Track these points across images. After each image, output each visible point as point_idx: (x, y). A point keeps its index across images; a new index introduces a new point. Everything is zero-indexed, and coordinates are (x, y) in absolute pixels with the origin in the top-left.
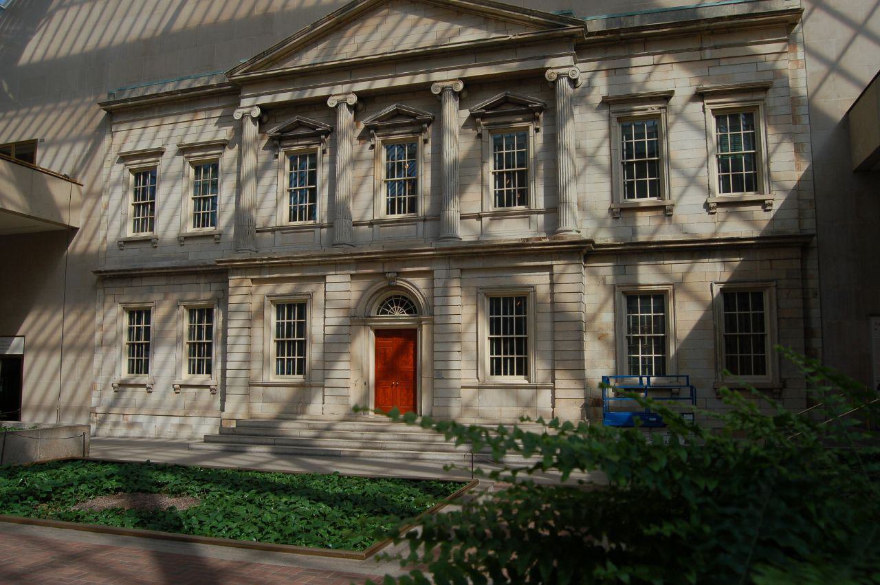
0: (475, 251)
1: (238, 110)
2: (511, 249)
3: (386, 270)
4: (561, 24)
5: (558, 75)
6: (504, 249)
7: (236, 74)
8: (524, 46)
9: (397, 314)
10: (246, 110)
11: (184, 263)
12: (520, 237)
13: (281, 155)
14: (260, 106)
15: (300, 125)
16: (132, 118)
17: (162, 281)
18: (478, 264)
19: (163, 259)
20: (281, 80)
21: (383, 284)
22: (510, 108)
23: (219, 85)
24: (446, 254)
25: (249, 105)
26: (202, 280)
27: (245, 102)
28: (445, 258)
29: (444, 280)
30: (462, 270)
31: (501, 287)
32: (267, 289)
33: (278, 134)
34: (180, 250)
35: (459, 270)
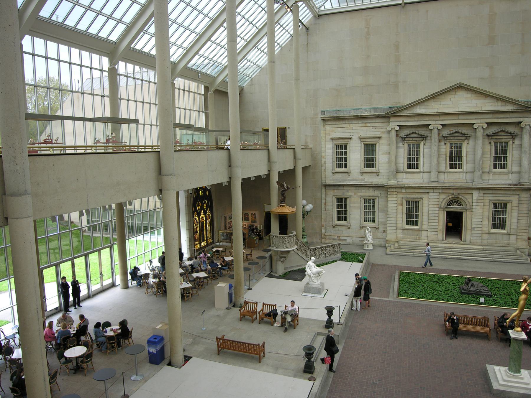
3: (454, 192)
7: (390, 114)
9: (455, 206)
10: (393, 127)
16: (334, 123)
17: (353, 188)
19: (353, 180)
21: (453, 196)
22: (503, 133)
25: (395, 124)
26: (371, 189)
32: (401, 196)
34: (360, 177)
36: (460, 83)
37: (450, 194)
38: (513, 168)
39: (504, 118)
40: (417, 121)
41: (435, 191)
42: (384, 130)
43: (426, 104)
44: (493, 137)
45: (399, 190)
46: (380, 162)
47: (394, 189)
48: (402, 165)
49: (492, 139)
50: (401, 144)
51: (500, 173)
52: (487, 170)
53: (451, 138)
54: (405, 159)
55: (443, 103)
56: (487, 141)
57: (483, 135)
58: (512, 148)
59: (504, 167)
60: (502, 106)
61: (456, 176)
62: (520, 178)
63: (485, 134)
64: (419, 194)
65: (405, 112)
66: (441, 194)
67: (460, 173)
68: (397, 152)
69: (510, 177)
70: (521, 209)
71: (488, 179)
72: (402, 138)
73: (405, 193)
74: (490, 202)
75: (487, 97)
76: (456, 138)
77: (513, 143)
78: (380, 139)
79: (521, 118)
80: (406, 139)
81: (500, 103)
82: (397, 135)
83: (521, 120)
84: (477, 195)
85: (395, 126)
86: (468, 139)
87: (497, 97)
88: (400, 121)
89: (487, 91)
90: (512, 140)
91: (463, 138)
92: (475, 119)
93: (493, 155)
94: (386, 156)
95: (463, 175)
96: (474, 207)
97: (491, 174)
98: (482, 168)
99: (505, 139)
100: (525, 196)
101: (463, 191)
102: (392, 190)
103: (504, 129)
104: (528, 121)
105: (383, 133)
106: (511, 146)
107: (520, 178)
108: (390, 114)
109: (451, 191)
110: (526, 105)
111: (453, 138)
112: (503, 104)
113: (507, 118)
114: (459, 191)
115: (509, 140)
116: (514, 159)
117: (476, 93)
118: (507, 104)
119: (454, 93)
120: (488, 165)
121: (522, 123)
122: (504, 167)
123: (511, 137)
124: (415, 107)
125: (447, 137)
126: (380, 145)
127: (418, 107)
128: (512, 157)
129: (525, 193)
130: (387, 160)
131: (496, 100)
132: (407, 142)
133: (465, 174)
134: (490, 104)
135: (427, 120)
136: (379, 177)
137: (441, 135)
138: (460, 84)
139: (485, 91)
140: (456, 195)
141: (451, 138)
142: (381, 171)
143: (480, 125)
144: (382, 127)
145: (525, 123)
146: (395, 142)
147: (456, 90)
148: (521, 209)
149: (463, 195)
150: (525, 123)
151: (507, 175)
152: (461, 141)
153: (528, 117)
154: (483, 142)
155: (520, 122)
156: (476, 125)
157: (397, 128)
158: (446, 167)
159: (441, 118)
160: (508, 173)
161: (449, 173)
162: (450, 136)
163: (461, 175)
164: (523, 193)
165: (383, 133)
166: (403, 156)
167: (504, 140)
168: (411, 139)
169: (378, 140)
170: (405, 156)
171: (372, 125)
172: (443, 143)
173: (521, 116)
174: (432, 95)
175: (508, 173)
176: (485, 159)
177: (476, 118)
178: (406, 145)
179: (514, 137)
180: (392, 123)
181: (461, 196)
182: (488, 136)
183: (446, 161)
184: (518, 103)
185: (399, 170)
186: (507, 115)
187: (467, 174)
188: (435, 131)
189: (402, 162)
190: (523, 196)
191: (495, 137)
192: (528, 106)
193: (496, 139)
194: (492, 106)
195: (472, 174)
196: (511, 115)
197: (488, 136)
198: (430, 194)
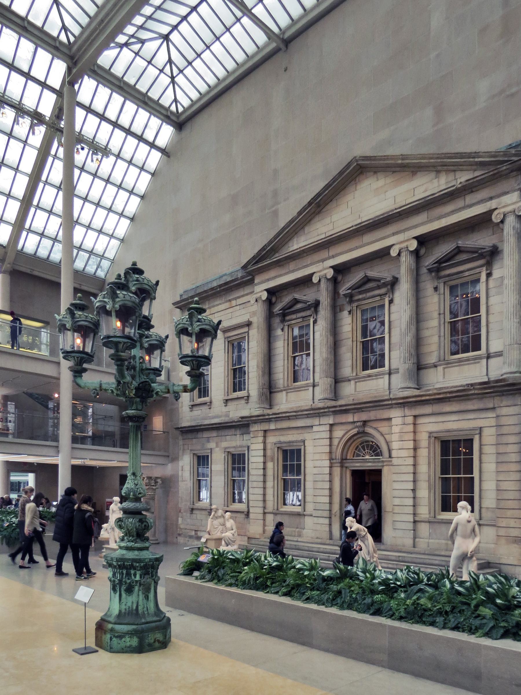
2: (454, 395)
4: (506, 159)
5: (505, 215)
6: (448, 395)
7: (249, 267)
11: (226, 419)
12: (465, 383)
18: (427, 409)
28: (401, 407)
30: (415, 417)
31: (448, 431)
37: (350, 427)
39: (453, 212)
40: (293, 271)
45: (265, 426)
49: (439, 278)
53: (360, 297)
56: (428, 286)
58: (487, 289)
64: (300, 431)
70: (502, 449)
73: (277, 433)
74: (429, 437)
77: (489, 275)
78: (251, 327)
79: (491, 198)
83: (493, 204)
88: (268, 280)
91: (383, 291)
96: (394, 454)
97: (440, 369)
99: (469, 270)
103: (460, 243)
104: (509, 202)
106: (484, 284)
108: (251, 268)
111: (364, 295)
114: (364, 416)
115: (478, 270)
121: (496, 213)
124: (290, 244)
129: (509, 403)
148: (502, 449)
149: (375, 425)
150: (502, 210)
151: (478, 365)
155: (490, 212)
162: (357, 290)
164: (504, 403)
167: (467, 274)
168: (294, 316)
171: (240, 301)
172: (345, 313)
173: (493, 194)
184: (476, 160)
188: (323, 285)
190: (505, 411)
191: (448, 272)
192: (501, 159)
193: (449, 275)
198: (315, 429)
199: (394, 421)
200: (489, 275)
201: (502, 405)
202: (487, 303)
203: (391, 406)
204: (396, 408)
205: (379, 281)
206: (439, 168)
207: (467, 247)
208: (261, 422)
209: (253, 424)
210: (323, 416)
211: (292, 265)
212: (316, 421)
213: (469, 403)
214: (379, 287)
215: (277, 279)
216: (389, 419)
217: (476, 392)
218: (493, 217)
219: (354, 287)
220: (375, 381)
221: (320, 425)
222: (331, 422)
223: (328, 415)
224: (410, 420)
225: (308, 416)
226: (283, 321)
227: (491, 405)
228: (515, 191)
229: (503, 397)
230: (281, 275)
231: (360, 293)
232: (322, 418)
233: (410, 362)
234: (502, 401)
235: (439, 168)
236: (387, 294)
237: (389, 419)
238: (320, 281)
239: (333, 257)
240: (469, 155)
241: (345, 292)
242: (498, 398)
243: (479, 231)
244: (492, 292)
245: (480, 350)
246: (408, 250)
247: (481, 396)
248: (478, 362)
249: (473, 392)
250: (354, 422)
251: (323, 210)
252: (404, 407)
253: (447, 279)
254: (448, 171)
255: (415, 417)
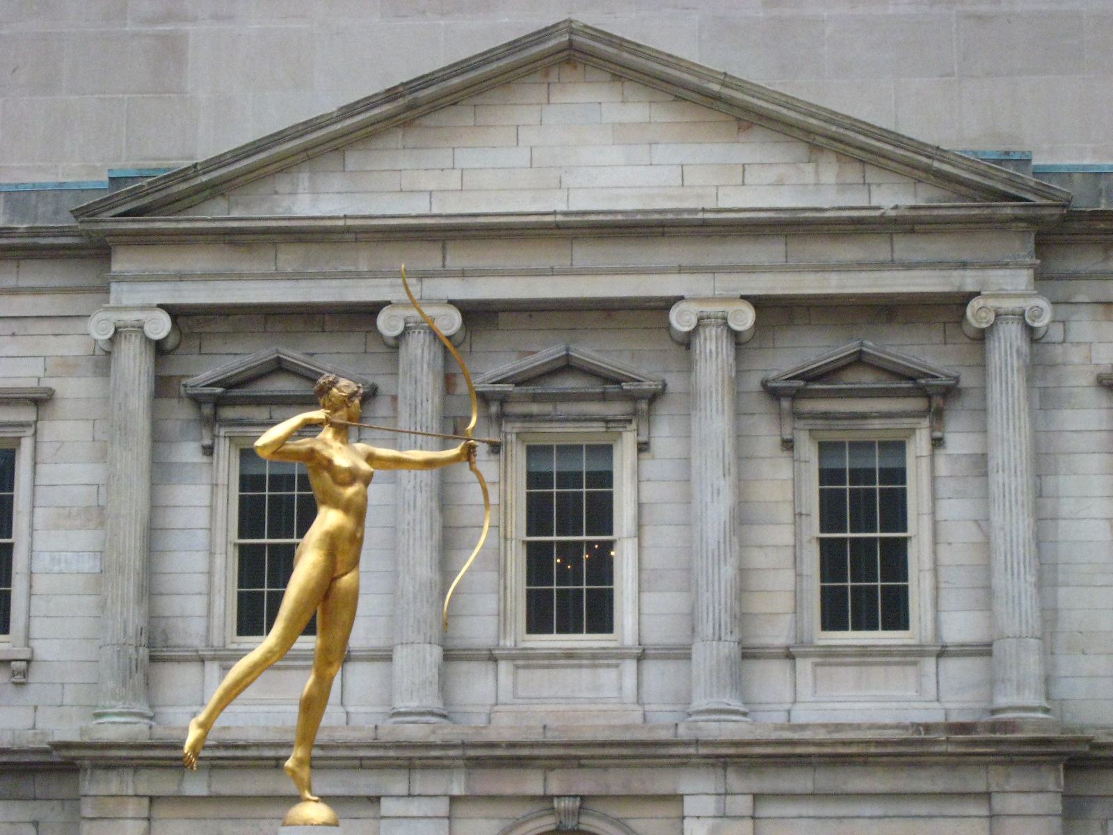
0: (799, 750)
1: (101, 315)
2: (890, 750)
3: (554, 788)
4: (1013, 191)
5: (997, 315)
7: (105, 216)
8: (912, 231)
10: (130, 317)
13: (223, 448)
14: (170, 310)
15: (279, 367)
18: (801, 781)
20: (231, 243)
22: (866, 379)
23: (33, 232)
24: (718, 757)
27: (122, 294)
28: (713, 765)
29: (710, 821)
30: (757, 797)
33: (219, 390)
35: (750, 798)
36: (568, 26)
37: (528, 809)
38: (944, 616)
40: (296, 276)
41: (427, 783)
42: (72, 346)
43: (353, 159)
44: (808, 406)
45: (164, 784)
46: (40, 584)
47: (128, 776)
48: (196, 605)
49: (798, 416)
50: (189, 452)
51: (864, 652)
52: (777, 635)
53: (535, 408)
54: (219, 561)
55: (466, 158)
56: (766, 433)
57: (738, 395)
58: (934, 479)
59: (897, 617)
60: (843, 186)
61: (576, 681)
62: (992, 683)
63: (754, 382)
65: (216, 214)
66: (461, 810)
67: (596, 658)
68: (155, 507)
69: (930, 685)
71: (788, 697)
72: (197, 400)
73: (210, 810)
75: (751, 125)
76: (564, 409)
77: (937, 443)
79: (964, 265)
80: (229, 413)
81: (829, 172)
82: (162, 386)
83: (967, 280)
84: (708, 805)
85: (143, 308)
86: (648, 417)
87: (808, 131)
88: (181, 277)
89: (739, 85)
90: (925, 423)
91: (616, 409)
92: (681, 270)
93: (813, 528)
94: (84, 538)
95: (620, 677)
97: (805, 666)
98: (742, 618)
100: (1030, 803)
101: (615, 781)
102: (113, 784)
103: (870, 346)
105: (68, 367)
106: (925, 464)
107: (992, 683)
108: (108, 223)
109: (533, 784)
110: (985, 176)
111: (547, 408)
112: (852, 173)
113: (881, 266)
114: (586, 783)
115: (906, 423)
116: (945, 555)
117: (678, 98)
118: (873, 175)
119: (538, 93)
120: (783, 603)
121: (974, 304)
122: (897, 617)
123: (916, 404)
124: (283, 184)
125: (504, 399)
126: (46, 451)
127: (304, 179)
128: (935, 542)
129: (1026, 783)
130: (89, 564)
131: (800, 150)
132: (237, 431)
133: (630, 666)
134: (771, 175)
135: (363, 267)
136: (33, 693)
137: (462, 388)
138: (572, 32)
139: (727, 80)
140: (567, 812)
141: (535, 408)
142: (43, 650)
143: (710, 309)
144: (62, 326)
145: (992, 303)
146: (141, 424)
147: (553, 77)
149: (616, 811)
150: (992, 303)
151: (910, 670)
152: (598, 427)
153: (1005, 266)
154: (740, 437)
155: (966, 298)
156: (680, 314)
157: (160, 327)
158: (502, 616)
159: (459, 257)
160: (911, 655)
161: (525, 659)
163: (607, 676)
164: (1016, 782)
165: (68, 367)
166: (202, 537)
167: (877, 424)
169: (27, 414)
170: (220, 540)
173: (966, 256)
174: (391, 95)
175: (911, 655)
176: (758, 559)
177: (685, 262)
178: (228, 466)
179: (938, 401)
180: (125, 286)
181: (604, 817)
182: (772, 393)
183: (502, 572)
184: (936, 164)
185: (175, 640)
186: (878, 249)
187: (653, 669)
188: (418, 350)
189: (199, 582)
190: (1013, 803)
192: (1000, 187)
193: (826, 416)
194: (779, 183)
195: (681, 664)
196: (904, 247)
197: (772, 393)
198: (388, 807)
199: (690, 806)
200: (937, 443)
201: (1007, 788)
202: (933, 513)
203: (682, 763)
204: (698, 766)
205: (618, 382)
206: (820, 140)
207: (880, 358)
208: (137, 768)
209: (100, 774)
210: (425, 767)
211: (289, 258)
212: (397, 784)
213: (924, 773)
214: (603, 398)
215: (222, 285)
216: (677, 798)
217: (951, 749)
218: (969, 311)
219: (519, 379)
220: (585, 671)
221: (410, 795)
222: (457, 789)
223: (448, 767)
224: (742, 804)
225: (362, 765)
226: (213, 421)
227: (980, 786)
228: (1020, 266)
229: (1011, 769)
230: (240, 277)
231: (535, 398)
232: (417, 776)
233: (733, 638)
234: (1008, 776)
235: (820, 140)
236: (630, 421)
237: (677, 798)
238: (406, 330)
239: (463, 274)
240: (920, 148)
241: (487, 388)
242: (1000, 769)
243: (906, 323)
244: (944, 488)
245: (905, 626)
246: (726, 324)
247: (954, 762)
248: (914, 664)
249: (942, 748)
250: (548, 798)
251: (426, 121)
252: (725, 766)
253: (820, 423)
254: (841, 155)
255: (757, 797)
